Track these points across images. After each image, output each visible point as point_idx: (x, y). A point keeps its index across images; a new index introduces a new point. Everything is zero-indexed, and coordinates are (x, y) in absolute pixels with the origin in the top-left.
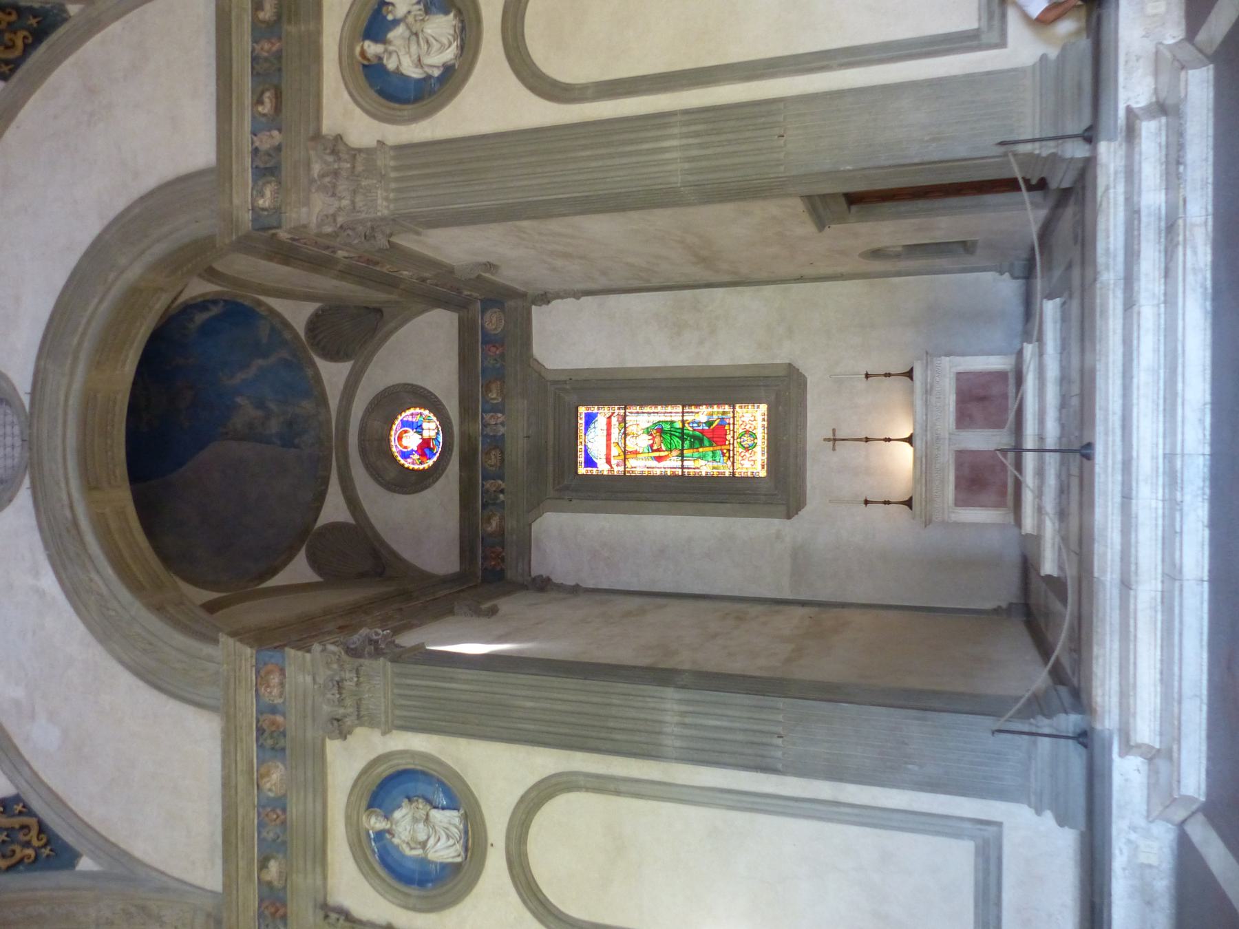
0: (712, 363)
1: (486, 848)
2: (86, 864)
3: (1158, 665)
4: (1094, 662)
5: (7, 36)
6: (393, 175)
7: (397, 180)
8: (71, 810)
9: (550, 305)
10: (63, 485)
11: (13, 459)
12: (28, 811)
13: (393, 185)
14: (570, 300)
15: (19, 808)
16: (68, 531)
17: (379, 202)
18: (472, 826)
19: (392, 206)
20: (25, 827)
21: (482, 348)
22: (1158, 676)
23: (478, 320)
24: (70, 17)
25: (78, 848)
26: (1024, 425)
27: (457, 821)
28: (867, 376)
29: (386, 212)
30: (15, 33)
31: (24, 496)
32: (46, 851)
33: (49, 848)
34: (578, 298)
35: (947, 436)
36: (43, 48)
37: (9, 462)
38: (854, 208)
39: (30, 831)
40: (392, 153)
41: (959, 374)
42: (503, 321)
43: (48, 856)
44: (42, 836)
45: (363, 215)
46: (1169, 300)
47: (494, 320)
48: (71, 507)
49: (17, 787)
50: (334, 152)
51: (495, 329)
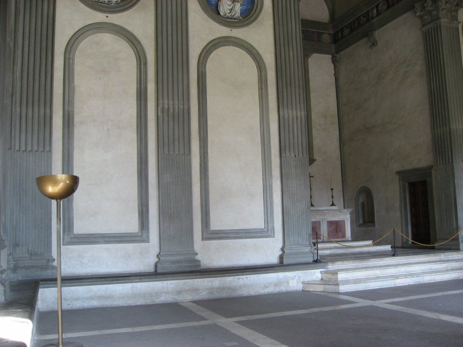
0: (313, 129)
1: (231, 28)
3: (360, 278)
4: (347, 261)
6: (451, 26)
7: (450, 27)
9: (332, 63)
13: (448, 25)
14: (333, 72)
17: (445, 19)
18: (234, 22)
19: (442, 24)
21: (316, 32)
22: (358, 278)
23: (326, 31)
26: (357, 242)
27: (237, 15)
28: (332, 189)
29: (441, 21)
34: (335, 75)
35: (325, 218)
38: (407, 184)
40: (457, 26)
41: (344, 221)
42: (326, 42)
45: (440, 12)
46: (453, 270)
47: (327, 38)
50: (457, 5)
51: (324, 39)
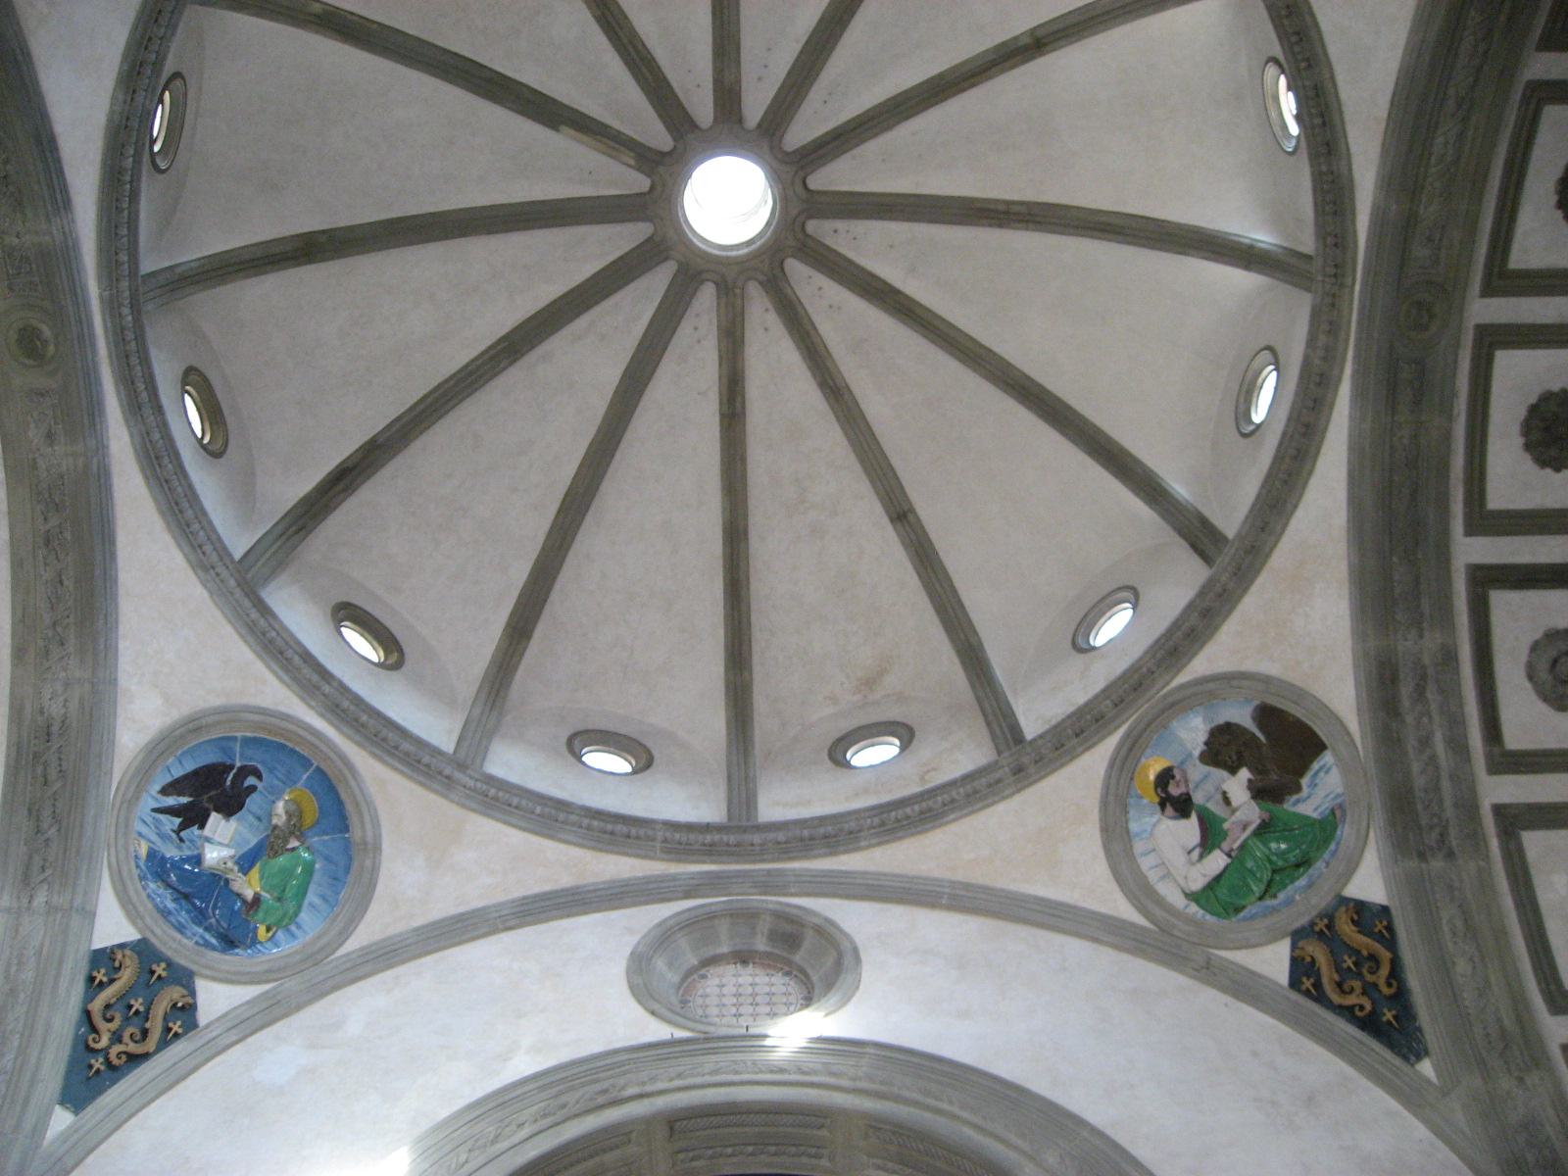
2: (62, 1119)
5: (1357, 984)
8: (152, 1100)
10: (678, 1083)
11: (718, 1016)
12: (168, 1038)
15: (176, 1028)
16: (605, 1091)
20: (145, 1033)
24: (1412, 1065)
25: (90, 1110)
30: (1363, 994)
31: (658, 1031)
32: (98, 1063)
33: (102, 1068)
36: (1352, 1030)
37: (714, 1011)
39: (136, 1042)
43: (91, 1067)
44: (124, 1058)
48: (641, 1096)
49: (207, 1026)
